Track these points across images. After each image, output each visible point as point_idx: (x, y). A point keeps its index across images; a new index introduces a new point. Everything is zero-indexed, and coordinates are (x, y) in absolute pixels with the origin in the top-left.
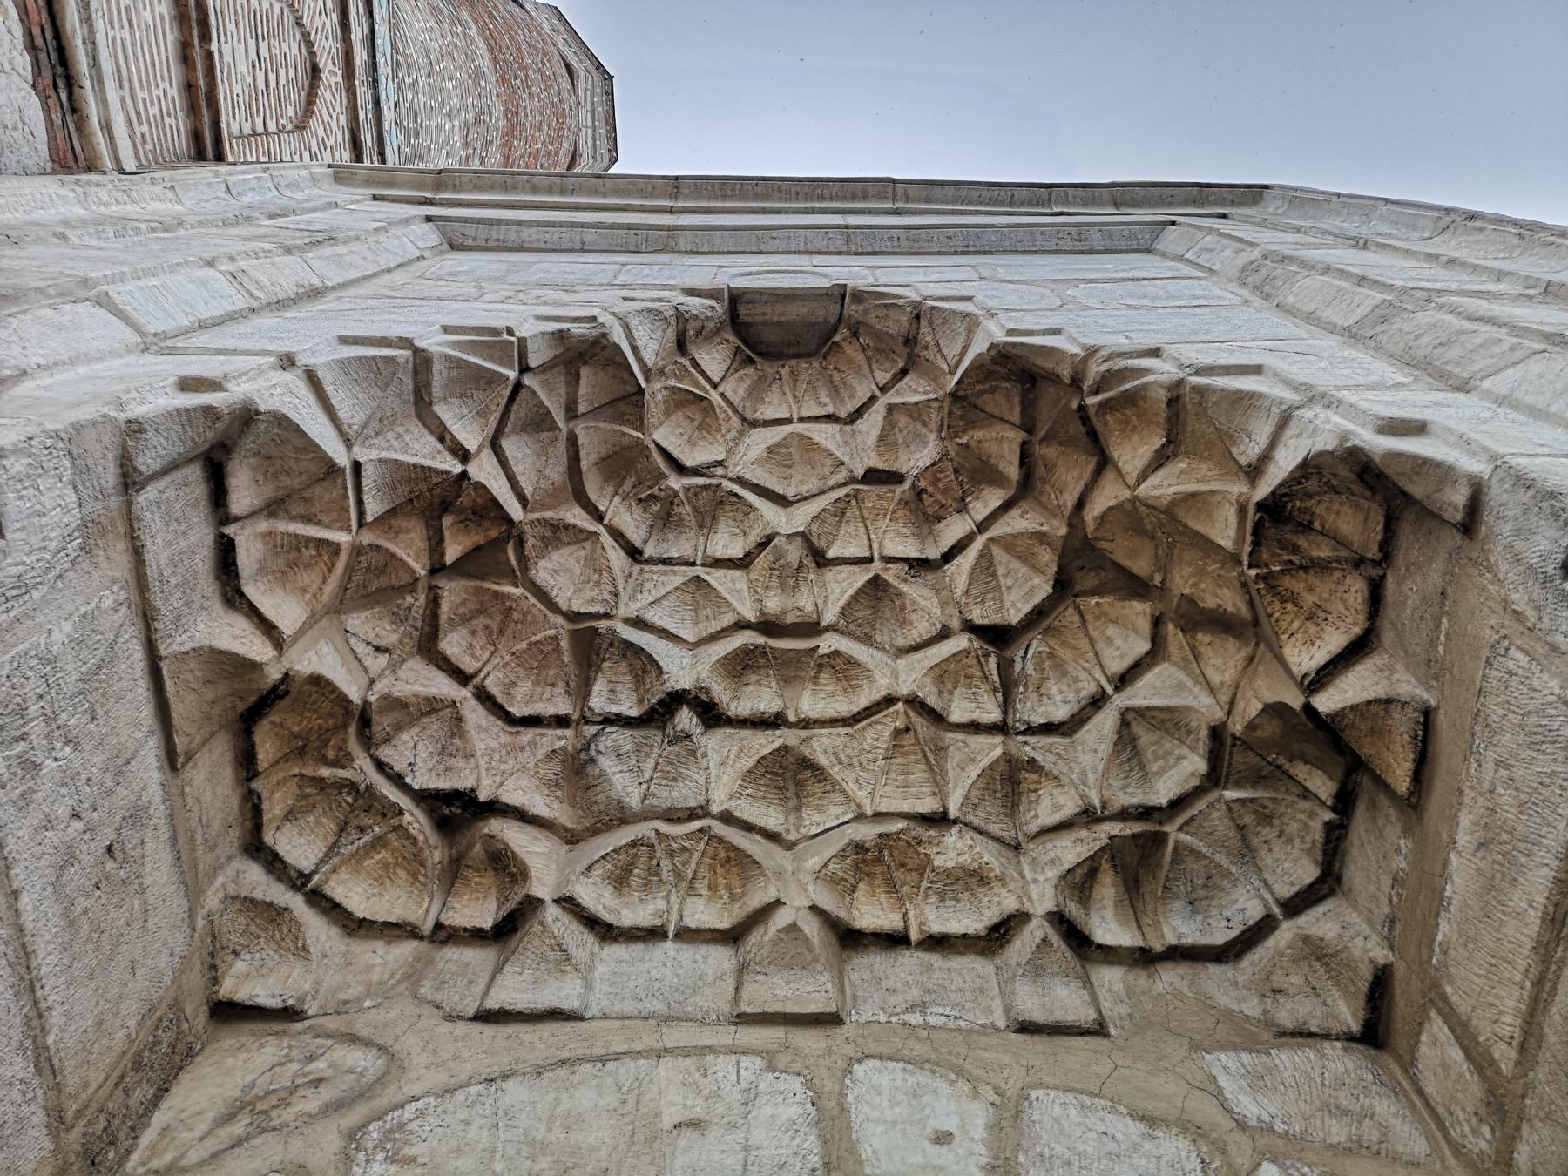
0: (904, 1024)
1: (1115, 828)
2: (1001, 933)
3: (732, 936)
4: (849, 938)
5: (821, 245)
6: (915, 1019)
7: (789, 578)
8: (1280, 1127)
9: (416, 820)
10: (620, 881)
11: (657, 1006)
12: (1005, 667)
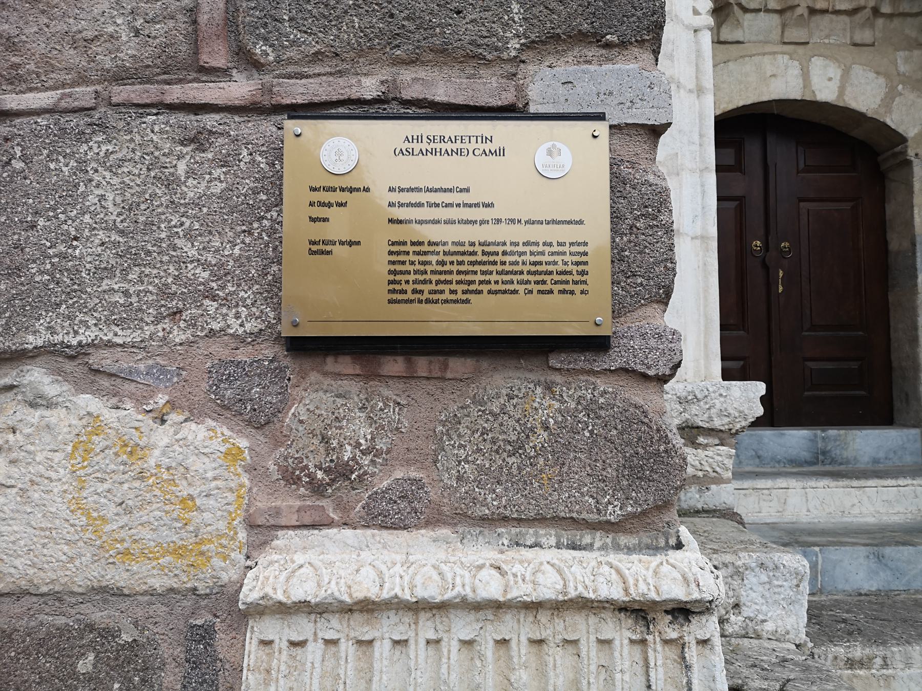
0: (824, 43)
3: (780, 12)
6: (826, 41)
8: (907, 74)
11: (761, 38)
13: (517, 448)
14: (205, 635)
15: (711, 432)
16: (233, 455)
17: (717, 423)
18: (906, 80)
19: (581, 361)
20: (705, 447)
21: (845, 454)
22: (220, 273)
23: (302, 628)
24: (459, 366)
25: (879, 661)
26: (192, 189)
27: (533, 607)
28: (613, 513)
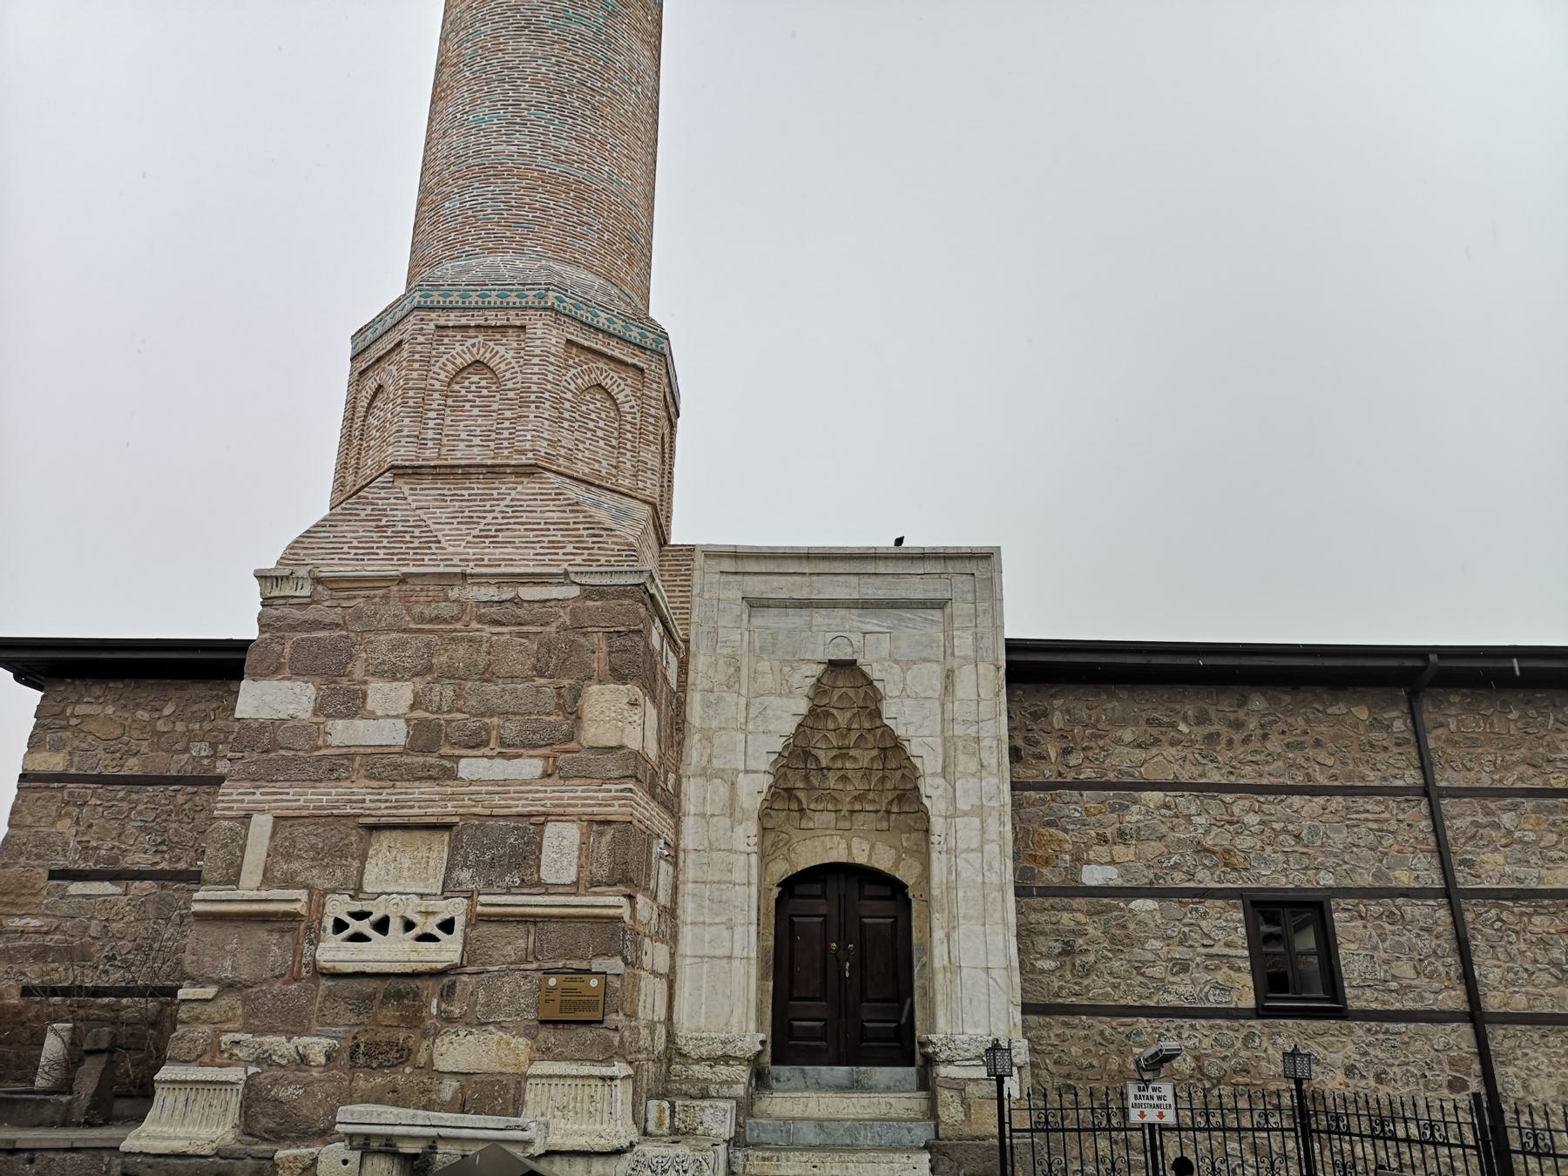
1: (898, 792)
2: (877, 812)
3: (836, 811)
4: (853, 811)
5: (852, 605)
7: (843, 737)
9: (782, 792)
10: (816, 802)
12: (885, 755)
13: (584, 1044)
14: (519, 1082)
15: (736, 1058)
16: (527, 1045)
17: (738, 1054)
18: (906, 850)
19: (597, 1026)
20: (732, 1066)
21: (870, 1083)
22: (528, 1006)
23: (538, 1081)
24: (573, 1026)
25: (775, 1158)
26: (524, 988)
27: (583, 1077)
28: (601, 1058)
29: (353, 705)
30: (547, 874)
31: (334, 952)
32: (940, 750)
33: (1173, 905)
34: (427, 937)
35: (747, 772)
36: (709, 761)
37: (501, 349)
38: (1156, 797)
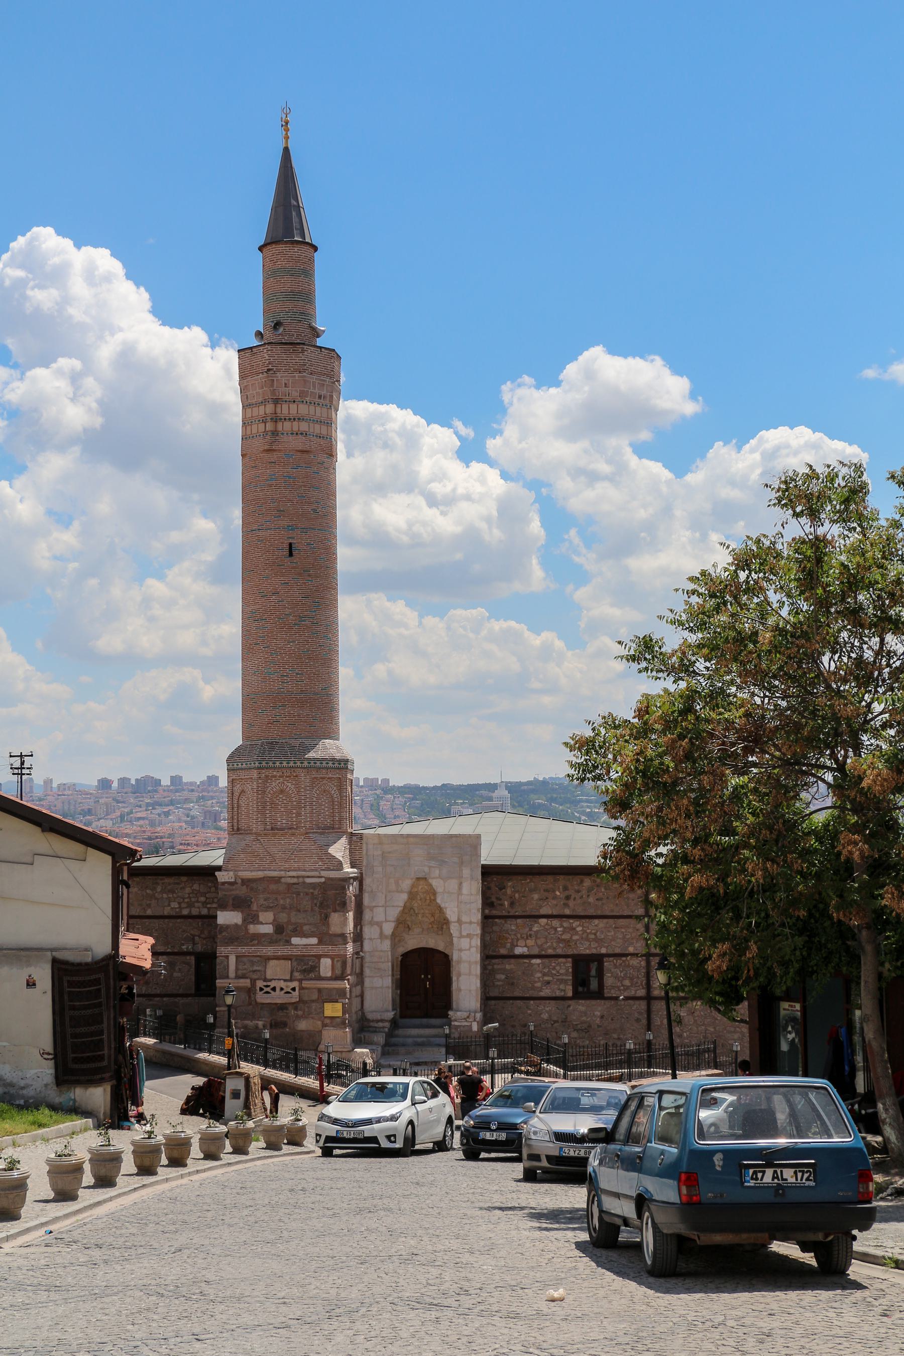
29: (255, 919)
30: (322, 974)
31: (261, 998)
32: (457, 914)
33: (546, 961)
34: (287, 993)
35: (386, 921)
36: (372, 918)
37: (289, 784)
38: (543, 921)
